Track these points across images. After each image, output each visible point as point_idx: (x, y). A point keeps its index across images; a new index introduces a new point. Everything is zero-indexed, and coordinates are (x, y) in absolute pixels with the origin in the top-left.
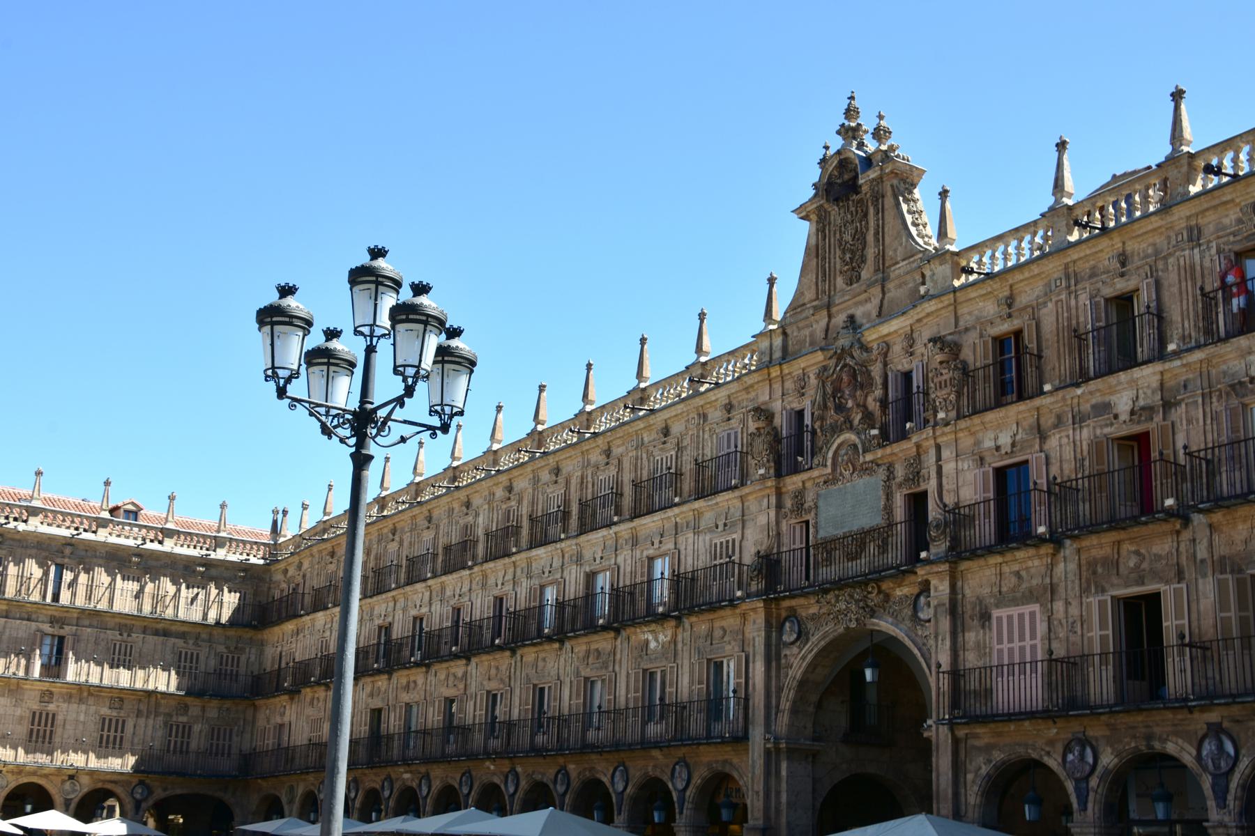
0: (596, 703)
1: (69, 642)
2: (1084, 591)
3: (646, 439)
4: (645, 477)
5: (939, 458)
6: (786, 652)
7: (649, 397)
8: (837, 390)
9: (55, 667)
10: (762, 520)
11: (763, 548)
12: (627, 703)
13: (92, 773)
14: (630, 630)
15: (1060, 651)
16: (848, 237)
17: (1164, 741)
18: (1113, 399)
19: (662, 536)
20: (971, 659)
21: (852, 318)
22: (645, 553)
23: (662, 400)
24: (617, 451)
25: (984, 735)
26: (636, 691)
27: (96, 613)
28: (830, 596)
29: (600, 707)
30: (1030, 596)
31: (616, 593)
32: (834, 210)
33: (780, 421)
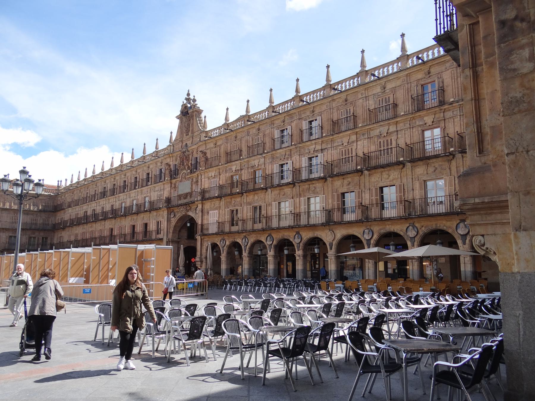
2: (225, 208)
5: (201, 178)
6: (172, 219)
8: (183, 160)
10: (168, 189)
11: (167, 196)
15: (220, 221)
16: (186, 125)
17: (237, 239)
18: (232, 167)
20: (205, 222)
21: (186, 144)
25: (206, 238)
28: (180, 207)
30: (216, 209)
31: (150, 202)
32: (184, 117)
33: (172, 167)
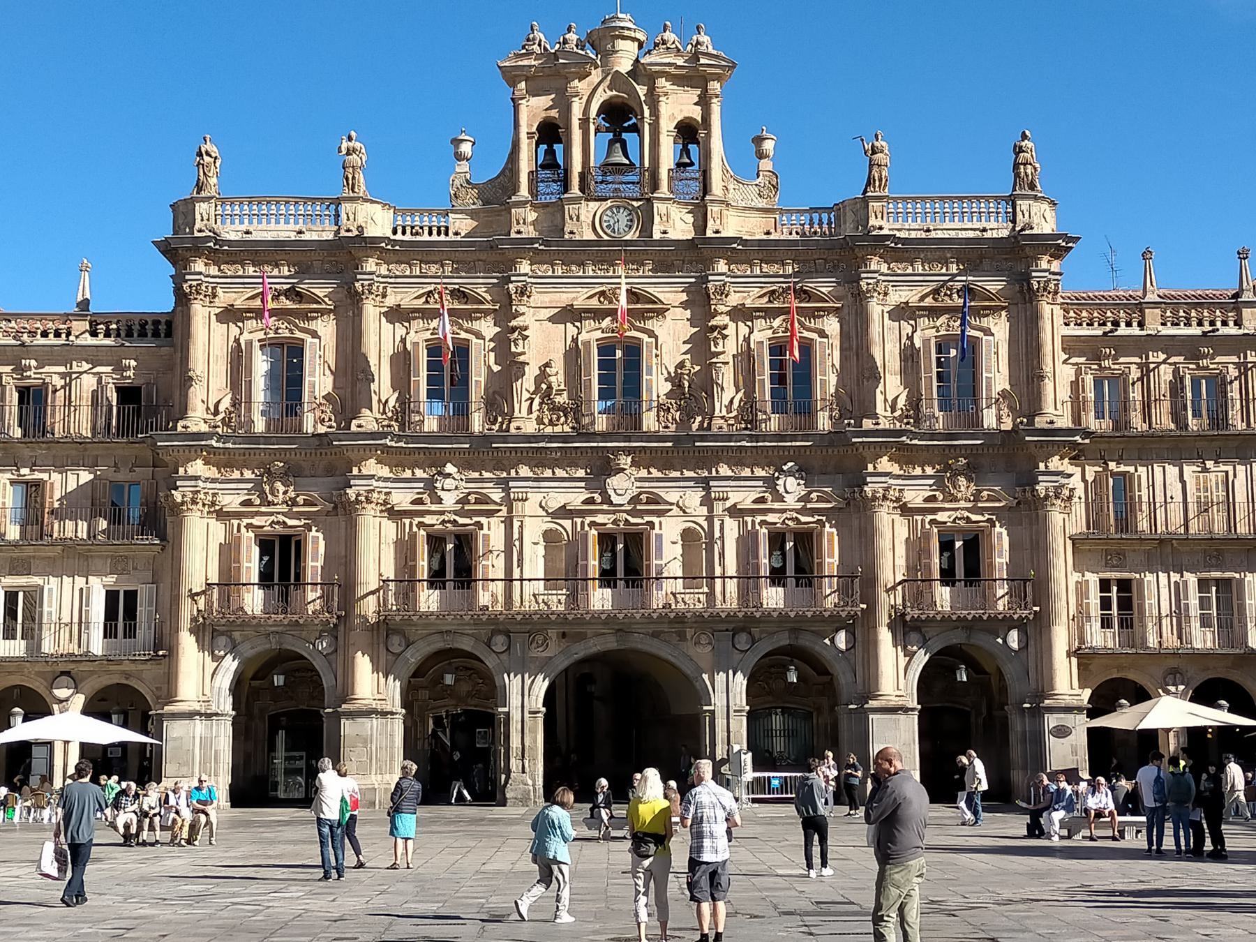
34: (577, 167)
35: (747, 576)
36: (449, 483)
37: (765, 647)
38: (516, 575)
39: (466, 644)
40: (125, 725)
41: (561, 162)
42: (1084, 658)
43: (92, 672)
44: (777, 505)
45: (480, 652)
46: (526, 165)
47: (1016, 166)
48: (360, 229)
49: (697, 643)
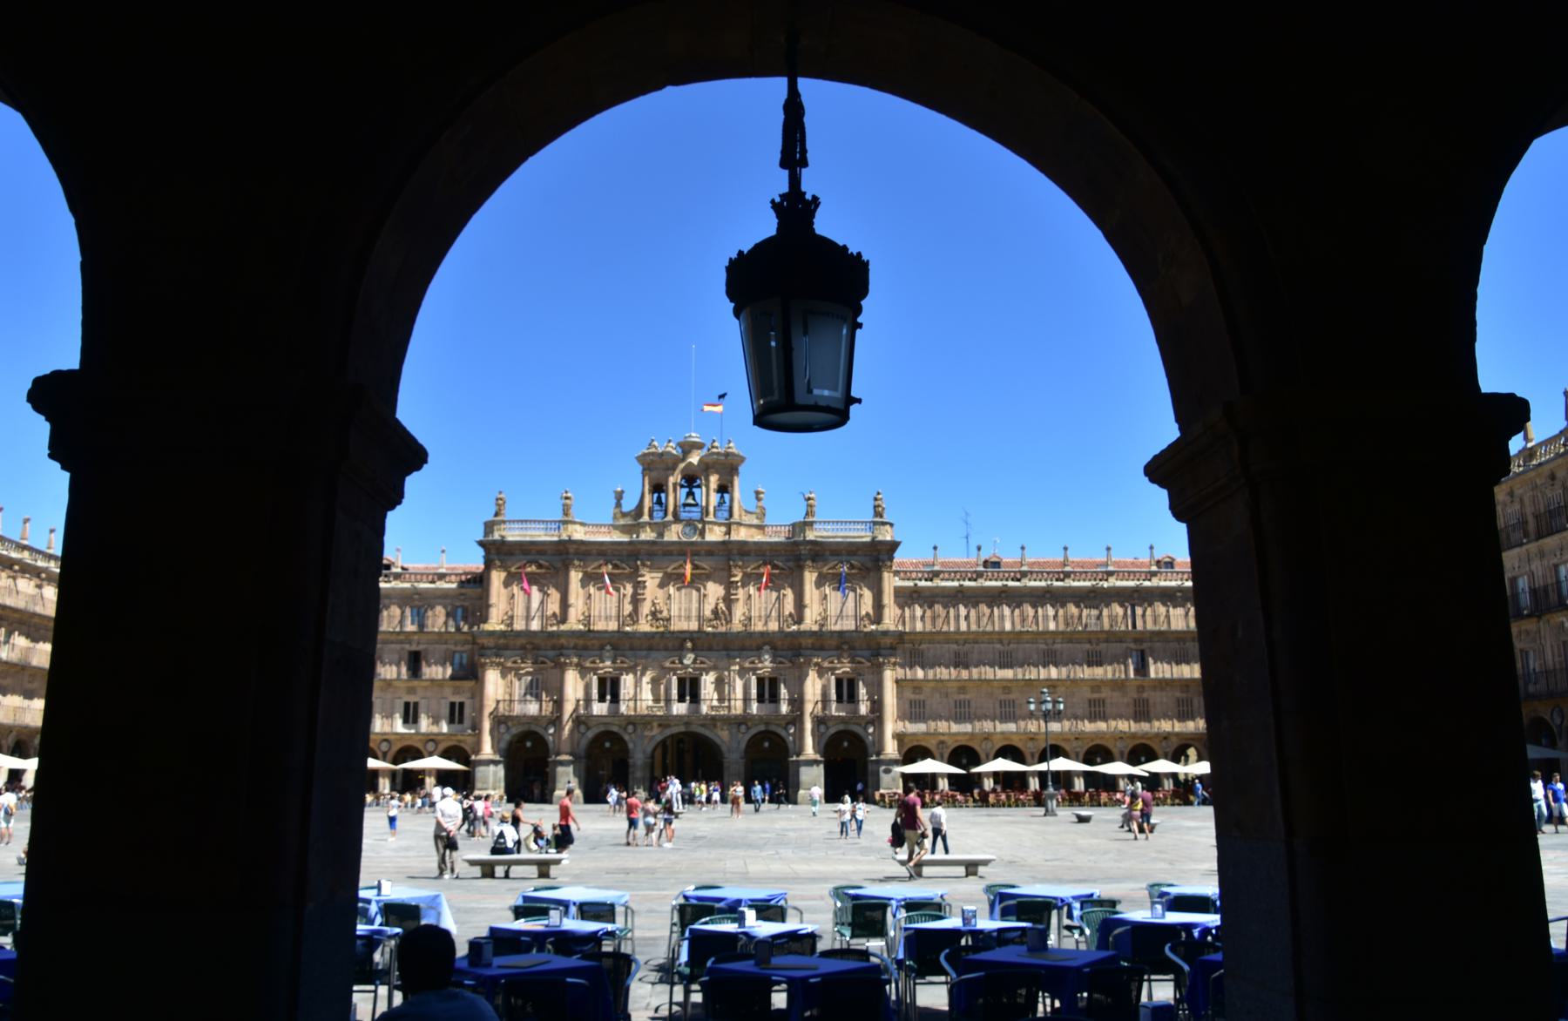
0: (1531, 667)
1: (1147, 652)
3: (1538, 482)
4: (1542, 510)
7: (1536, 453)
9: (1142, 669)
12: (1554, 665)
13: (1178, 735)
14: (1547, 616)
19: (1562, 550)
22: (1551, 563)
23: (1545, 455)
24: (1518, 492)
26: (1560, 656)
27: (1160, 633)
29: (1534, 669)
34: (671, 508)
35: (746, 700)
36: (608, 654)
37: (753, 731)
38: (638, 698)
39: (615, 729)
40: (458, 762)
41: (663, 500)
42: (899, 737)
43: (443, 740)
44: (760, 665)
45: (621, 732)
46: (647, 503)
47: (875, 507)
48: (570, 537)
49: (722, 729)
